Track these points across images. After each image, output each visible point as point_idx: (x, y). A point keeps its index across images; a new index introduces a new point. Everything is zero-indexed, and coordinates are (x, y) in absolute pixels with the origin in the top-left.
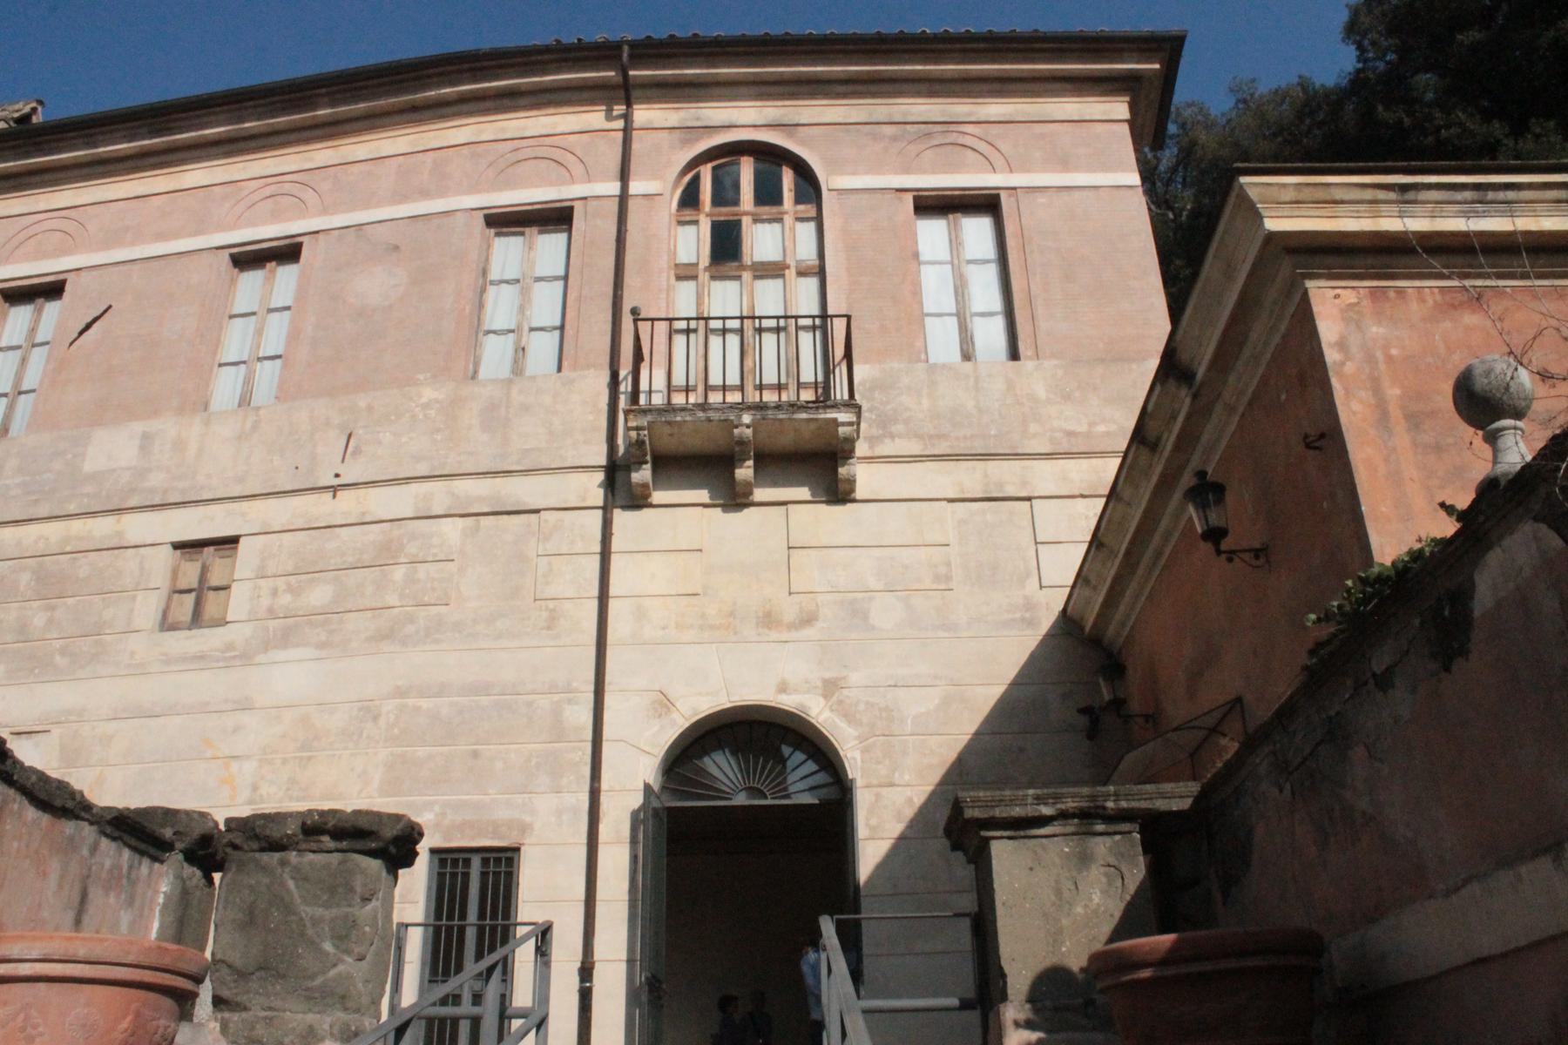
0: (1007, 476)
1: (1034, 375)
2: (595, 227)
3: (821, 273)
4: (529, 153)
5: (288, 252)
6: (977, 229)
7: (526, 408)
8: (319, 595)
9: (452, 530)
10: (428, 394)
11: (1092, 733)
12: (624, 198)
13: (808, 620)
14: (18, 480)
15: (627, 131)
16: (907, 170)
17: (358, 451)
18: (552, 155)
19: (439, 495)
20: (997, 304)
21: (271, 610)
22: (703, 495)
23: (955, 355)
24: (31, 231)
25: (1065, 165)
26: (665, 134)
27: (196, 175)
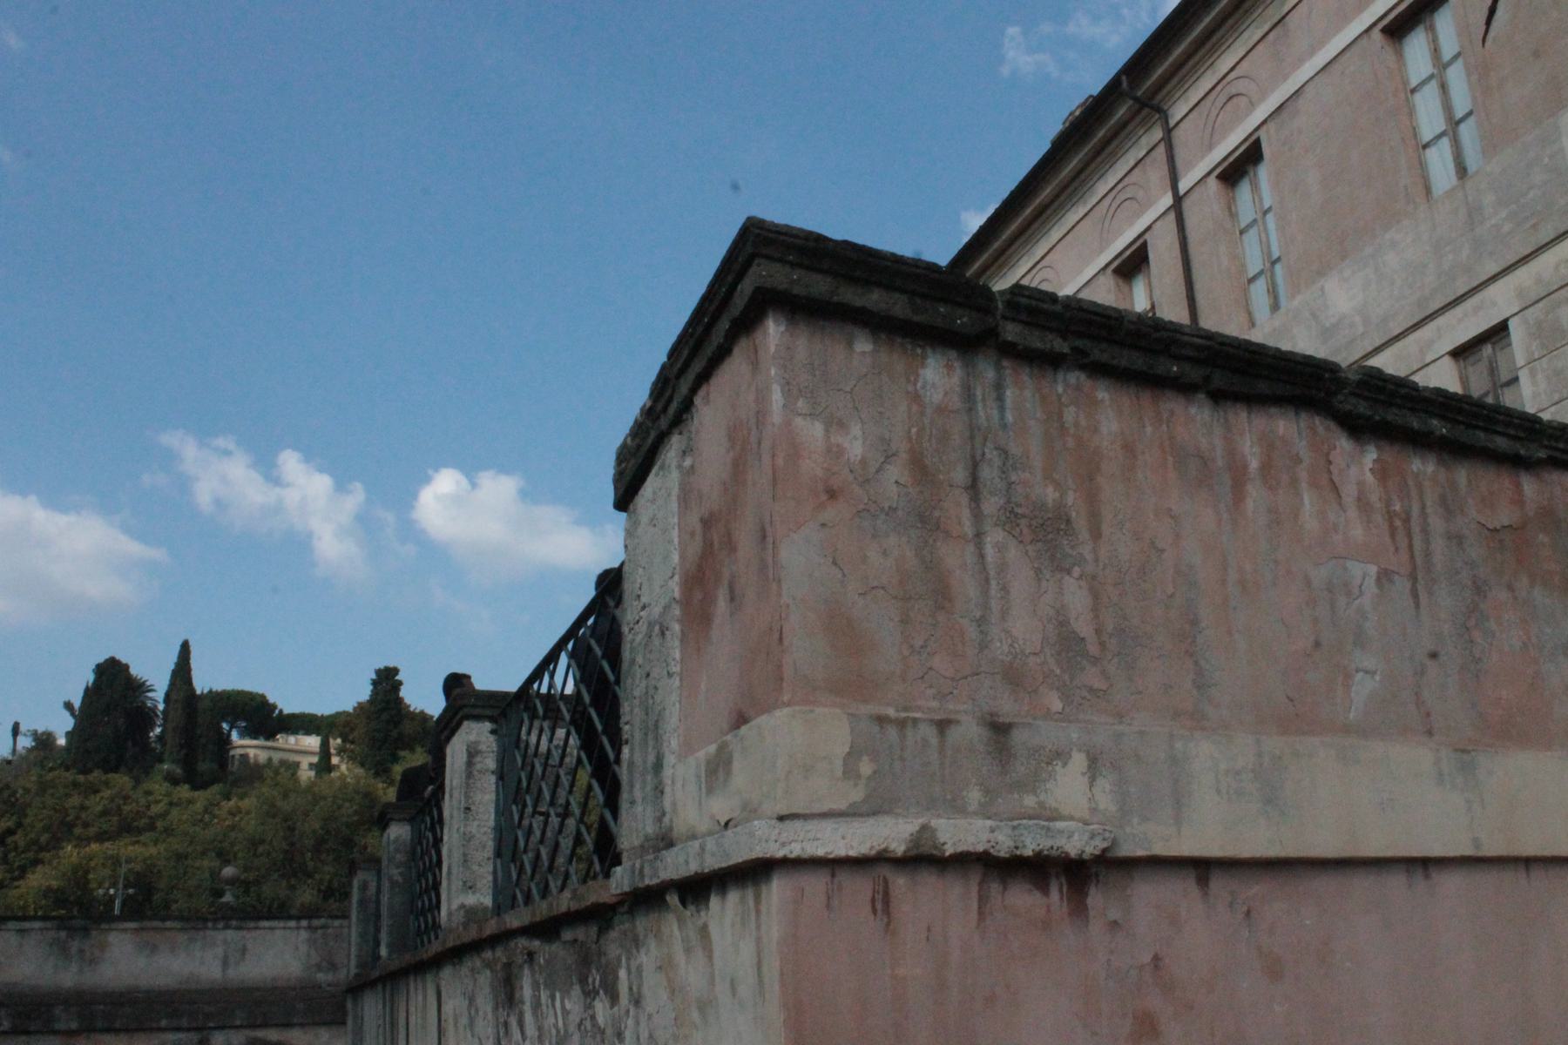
14: (1504, 214)
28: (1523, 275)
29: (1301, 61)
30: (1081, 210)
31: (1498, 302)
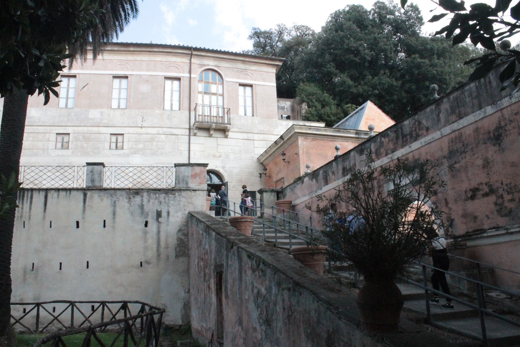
0: (250, 136)
1: (256, 119)
2: (185, 82)
3: (223, 95)
5: (126, 77)
6: (248, 89)
8: (141, 146)
9: (163, 136)
10: (157, 112)
11: (260, 177)
13: (220, 157)
15: (190, 63)
16: (238, 78)
17: (145, 121)
19: (161, 131)
20: (251, 105)
21: (132, 148)
23: (243, 114)
25: (264, 80)
28: (75, 128)
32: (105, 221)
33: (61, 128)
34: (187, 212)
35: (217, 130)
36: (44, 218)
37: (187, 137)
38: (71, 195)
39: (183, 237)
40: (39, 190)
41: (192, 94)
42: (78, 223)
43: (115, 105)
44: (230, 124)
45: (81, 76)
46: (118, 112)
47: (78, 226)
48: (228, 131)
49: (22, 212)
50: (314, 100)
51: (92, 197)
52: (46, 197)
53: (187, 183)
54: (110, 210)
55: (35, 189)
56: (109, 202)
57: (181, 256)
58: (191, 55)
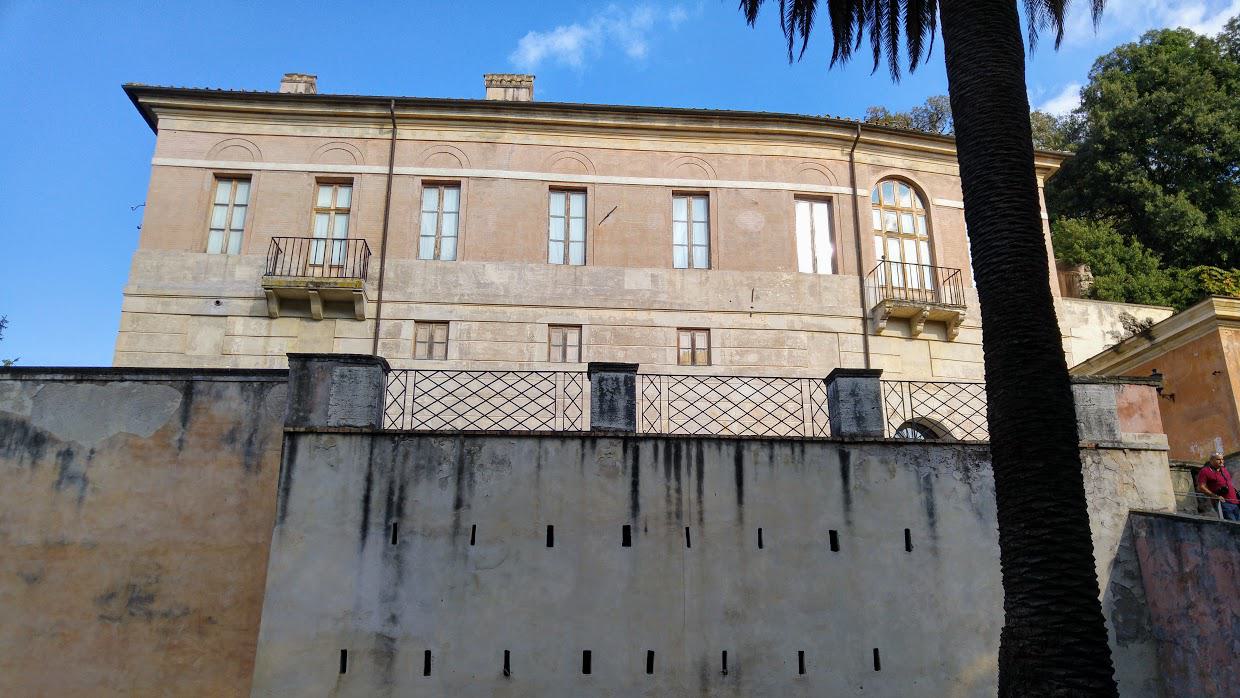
2: (844, 208)
4: (809, 165)
7: (826, 288)
9: (803, 336)
12: (854, 196)
17: (758, 298)
18: (823, 171)
22: (898, 333)
24: (560, 155)
26: (865, 166)
27: (645, 143)
28: (593, 313)
29: (499, 167)
30: (299, 131)
31: (580, 316)
32: (907, 532)
33: (560, 311)
34: (1125, 512)
35: (931, 323)
36: (740, 519)
37: (860, 339)
38: (807, 457)
39: (1127, 584)
40: (719, 440)
41: (862, 236)
42: (833, 535)
43: (680, 257)
44: (965, 307)
45: (598, 189)
46: (692, 279)
47: (835, 547)
48: (957, 325)
49: (679, 500)
50: (1109, 258)
51: (862, 464)
52: (739, 461)
53: (1111, 431)
54: (918, 499)
55: (709, 439)
56: (913, 477)
57: (1134, 638)
58: (856, 141)
